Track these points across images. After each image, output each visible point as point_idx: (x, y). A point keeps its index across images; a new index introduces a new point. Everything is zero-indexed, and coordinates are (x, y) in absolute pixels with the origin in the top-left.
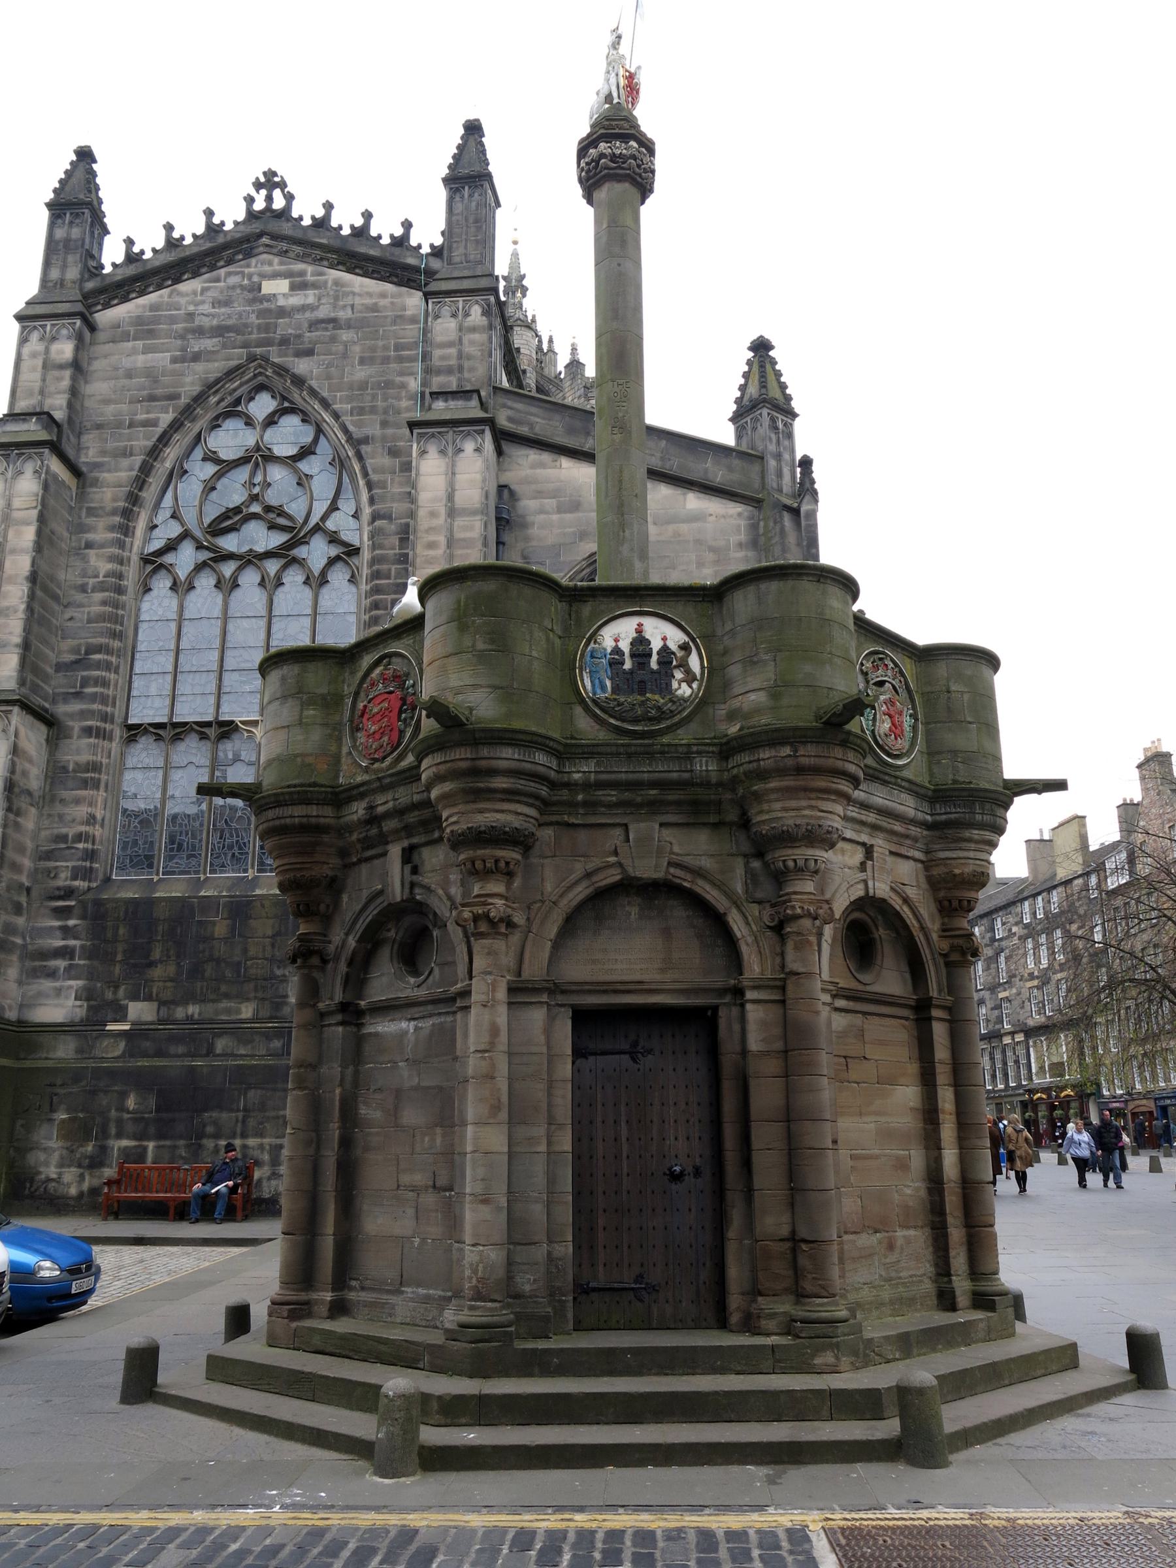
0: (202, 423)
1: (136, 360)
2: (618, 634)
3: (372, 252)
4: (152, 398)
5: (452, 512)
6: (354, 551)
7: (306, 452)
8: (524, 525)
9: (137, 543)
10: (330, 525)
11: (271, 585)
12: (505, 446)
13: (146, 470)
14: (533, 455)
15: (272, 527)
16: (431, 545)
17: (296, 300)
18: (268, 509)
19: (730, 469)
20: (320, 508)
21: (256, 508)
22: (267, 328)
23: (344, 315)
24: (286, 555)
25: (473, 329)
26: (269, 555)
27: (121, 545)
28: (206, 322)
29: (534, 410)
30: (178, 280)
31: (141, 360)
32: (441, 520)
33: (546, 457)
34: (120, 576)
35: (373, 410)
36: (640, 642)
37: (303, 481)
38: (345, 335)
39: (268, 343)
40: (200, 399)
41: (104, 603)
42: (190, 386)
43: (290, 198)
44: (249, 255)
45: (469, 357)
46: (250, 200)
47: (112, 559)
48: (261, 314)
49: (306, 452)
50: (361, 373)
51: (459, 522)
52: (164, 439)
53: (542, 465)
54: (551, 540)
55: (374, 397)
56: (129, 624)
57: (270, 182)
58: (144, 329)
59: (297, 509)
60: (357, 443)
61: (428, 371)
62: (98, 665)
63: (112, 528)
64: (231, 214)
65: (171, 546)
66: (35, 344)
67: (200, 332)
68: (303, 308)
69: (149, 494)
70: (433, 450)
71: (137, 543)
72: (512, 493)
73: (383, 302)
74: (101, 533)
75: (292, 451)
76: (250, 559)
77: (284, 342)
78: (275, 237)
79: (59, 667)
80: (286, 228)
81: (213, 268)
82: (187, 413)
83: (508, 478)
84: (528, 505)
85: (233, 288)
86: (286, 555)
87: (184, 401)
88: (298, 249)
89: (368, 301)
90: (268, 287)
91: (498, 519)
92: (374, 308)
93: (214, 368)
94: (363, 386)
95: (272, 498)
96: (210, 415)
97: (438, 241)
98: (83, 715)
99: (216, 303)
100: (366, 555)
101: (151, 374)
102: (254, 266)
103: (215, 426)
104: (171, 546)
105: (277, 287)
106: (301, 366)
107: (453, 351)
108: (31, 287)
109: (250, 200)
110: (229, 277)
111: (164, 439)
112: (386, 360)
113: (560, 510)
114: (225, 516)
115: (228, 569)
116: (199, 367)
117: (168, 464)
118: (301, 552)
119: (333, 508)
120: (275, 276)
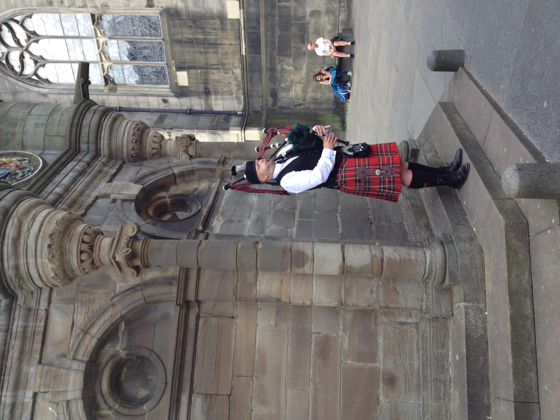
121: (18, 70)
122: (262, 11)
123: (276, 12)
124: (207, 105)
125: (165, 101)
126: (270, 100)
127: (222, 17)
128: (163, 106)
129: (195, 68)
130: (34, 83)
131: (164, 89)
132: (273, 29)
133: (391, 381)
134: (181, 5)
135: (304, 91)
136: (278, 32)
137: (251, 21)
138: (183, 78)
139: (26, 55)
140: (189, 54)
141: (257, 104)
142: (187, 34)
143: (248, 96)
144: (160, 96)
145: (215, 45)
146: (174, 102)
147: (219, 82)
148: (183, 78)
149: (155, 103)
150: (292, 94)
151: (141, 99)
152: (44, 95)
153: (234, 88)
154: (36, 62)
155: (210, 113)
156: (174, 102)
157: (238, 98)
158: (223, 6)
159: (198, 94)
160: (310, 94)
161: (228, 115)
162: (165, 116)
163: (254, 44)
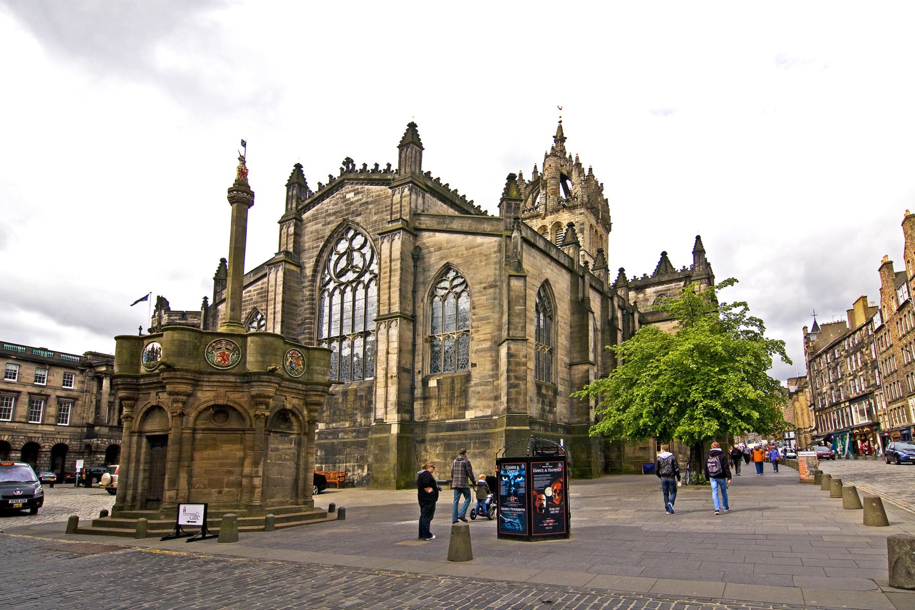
0: (333, 244)
1: (315, 228)
4: (318, 239)
5: (391, 261)
6: (376, 276)
7: (363, 246)
11: (354, 290)
13: (317, 261)
15: (354, 272)
16: (385, 273)
17: (356, 198)
18: (353, 267)
19: (492, 225)
22: (348, 209)
24: (358, 280)
26: (353, 281)
27: (312, 286)
28: (331, 211)
31: (314, 228)
37: (363, 255)
38: (370, 206)
40: (331, 236)
42: (327, 233)
43: (354, 166)
44: (342, 187)
47: (310, 290)
48: (346, 205)
49: (363, 246)
50: (375, 218)
52: (322, 251)
58: (315, 218)
61: (391, 214)
62: (308, 323)
64: (337, 174)
67: (330, 215)
68: (358, 200)
70: (385, 241)
74: (307, 284)
75: (359, 246)
76: (349, 283)
77: (353, 212)
79: (299, 325)
80: (352, 176)
82: (328, 241)
86: (358, 280)
90: (348, 196)
91: (413, 258)
92: (379, 195)
93: (332, 226)
94: (376, 221)
98: (305, 339)
101: (317, 231)
102: (344, 190)
103: (337, 244)
105: (350, 196)
106: (358, 219)
109: (342, 169)
110: (337, 195)
112: (382, 212)
114: (341, 271)
115: (342, 288)
116: (330, 226)
118: (362, 279)
120: (350, 192)
122: (468, 432)
123: (468, 441)
125: (419, 372)
126: (419, 439)
127: (466, 408)
128: (416, 371)
131: (427, 371)
132: (459, 439)
134: (473, 383)
136: (457, 442)
137: (463, 426)
138: (433, 383)
140: (446, 387)
142: (457, 386)
145: (451, 404)
146: (419, 378)
149: (418, 366)
151: (421, 358)
152: (422, 300)
155: (413, 399)
156: (419, 378)
158: (472, 409)
161: (411, 412)
163: (452, 427)
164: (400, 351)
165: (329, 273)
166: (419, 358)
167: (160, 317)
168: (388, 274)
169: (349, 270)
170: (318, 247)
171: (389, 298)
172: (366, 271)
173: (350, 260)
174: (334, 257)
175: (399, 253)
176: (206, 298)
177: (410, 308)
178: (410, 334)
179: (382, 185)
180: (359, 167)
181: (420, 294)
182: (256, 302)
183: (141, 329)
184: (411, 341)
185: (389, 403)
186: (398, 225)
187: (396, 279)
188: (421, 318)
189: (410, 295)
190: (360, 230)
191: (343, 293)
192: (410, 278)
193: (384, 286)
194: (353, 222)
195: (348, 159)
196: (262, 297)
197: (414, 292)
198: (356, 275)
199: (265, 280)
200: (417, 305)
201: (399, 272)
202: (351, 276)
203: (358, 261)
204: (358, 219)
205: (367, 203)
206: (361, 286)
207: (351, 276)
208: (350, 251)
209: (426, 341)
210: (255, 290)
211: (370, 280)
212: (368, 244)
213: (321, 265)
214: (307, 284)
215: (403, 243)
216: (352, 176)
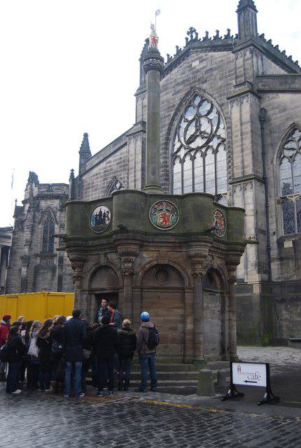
0: (182, 111)
2: (97, 211)
3: (220, 43)
5: (241, 124)
7: (209, 112)
8: (269, 120)
9: (170, 152)
10: (218, 134)
11: (204, 156)
12: (261, 95)
13: (169, 129)
14: (271, 95)
16: (237, 136)
17: (201, 66)
18: (201, 133)
20: (215, 128)
21: (198, 134)
22: (195, 77)
23: (213, 66)
25: (248, 60)
26: (202, 147)
27: (165, 153)
28: (179, 81)
29: (269, 80)
30: (172, 70)
32: (239, 127)
33: (275, 95)
34: (166, 162)
35: (224, 94)
36: (101, 212)
37: (210, 121)
38: (215, 72)
39: (195, 82)
40: (180, 104)
41: (163, 171)
42: (177, 101)
43: (197, 34)
44: (188, 56)
45: (247, 69)
46: (187, 39)
47: (164, 158)
49: (209, 112)
50: (220, 83)
51: (244, 126)
52: (173, 119)
53: (274, 98)
54: (278, 123)
55: (224, 90)
56: (170, 175)
57: (192, 31)
59: (209, 131)
60: (221, 106)
63: (163, 149)
64: (182, 45)
65: (179, 150)
66: (140, 102)
67: (178, 84)
68: (203, 68)
69: (171, 137)
70: (235, 105)
71: (170, 152)
72: (265, 110)
73: (224, 58)
74: (161, 151)
76: (198, 149)
77: (199, 80)
78: (194, 48)
80: (196, 44)
81: (180, 63)
82: (178, 110)
83: (262, 106)
84: (270, 112)
85: (185, 68)
86: (207, 145)
87: (176, 106)
88: (200, 50)
89: (220, 59)
91: (260, 120)
92: (222, 61)
93: (182, 95)
94: (221, 87)
95: (202, 130)
96: (184, 108)
97: (237, 33)
99: (182, 74)
100: (227, 140)
101: (168, 101)
102: (189, 59)
103: (186, 111)
104: (179, 150)
105: (196, 64)
106: (204, 86)
107: (242, 69)
108: (137, 85)
109: (187, 39)
110: (184, 64)
111: (173, 119)
112: (226, 77)
113: (280, 112)
114: (190, 138)
115: (192, 153)
117: (175, 126)
118: (211, 144)
119: (218, 127)
120: (196, 59)
121: (286, 146)
124: (274, 259)
125: (274, 233)
128: (271, 232)
129: (295, 252)
130: (279, 156)
131: (282, 233)
133: (166, 347)
135: (286, 319)
138: (288, 244)
139: (295, 152)
141: (277, 290)
143: (281, 284)
144: (277, 230)
146: (274, 239)
147: (288, 266)
148: (288, 244)
149: (273, 227)
150: (284, 312)
151: (274, 218)
153: (285, 275)
154: (291, 157)
155: (269, 261)
156: (274, 239)
157: (279, 278)
159: (280, 253)
160: (284, 324)
161: (269, 272)
162: (265, 235)
164: (256, 213)
165: (179, 140)
166: (272, 220)
167: (32, 190)
168: (240, 137)
169: (197, 136)
170: (169, 115)
171: (243, 161)
172: (214, 136)
173: (198, 127)
174: (184, 125)
175: (248, 116)
176: (72, 170)
177: (261, 170)
178: (263, 196)
179: (224, 50)
180: (201, 36)
181: (269, 156)
182: (116, 172)
183: (16, 201)
184: (264, 203)
185: (249, 264)
186: (245, 88)
187: (248, 142)
188: (272, 179)
189: (260, 157)
190: (206, 96)
191: (193, 158)
192: (259, 141)
193: (237, 150)
194: (200, 89)
195: (191, 28)
196: (121, 167)
197: (264, 154)
198: (204, 141)
199: (124, 150)
200: (267, 167)
201: (249, 136)
202: (199, 142)
203: (205, 127)
204: (204, 86)
205: (212, 69)
206: (210, 152)
207: (199, 142)
208: (198, 118)
209: (278, 202)
210: (115, 161)
211: (219, 145)
212: (215, 110)
213: (173, 132)
214: (161, 151)
215: (251, 106)
216: (196, 44)
